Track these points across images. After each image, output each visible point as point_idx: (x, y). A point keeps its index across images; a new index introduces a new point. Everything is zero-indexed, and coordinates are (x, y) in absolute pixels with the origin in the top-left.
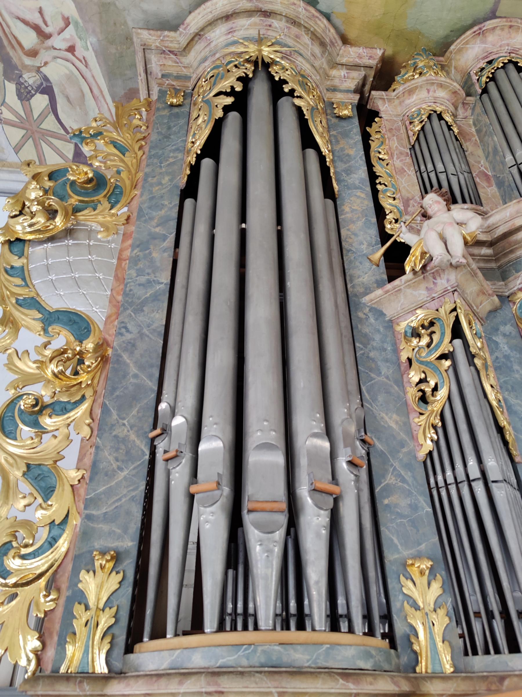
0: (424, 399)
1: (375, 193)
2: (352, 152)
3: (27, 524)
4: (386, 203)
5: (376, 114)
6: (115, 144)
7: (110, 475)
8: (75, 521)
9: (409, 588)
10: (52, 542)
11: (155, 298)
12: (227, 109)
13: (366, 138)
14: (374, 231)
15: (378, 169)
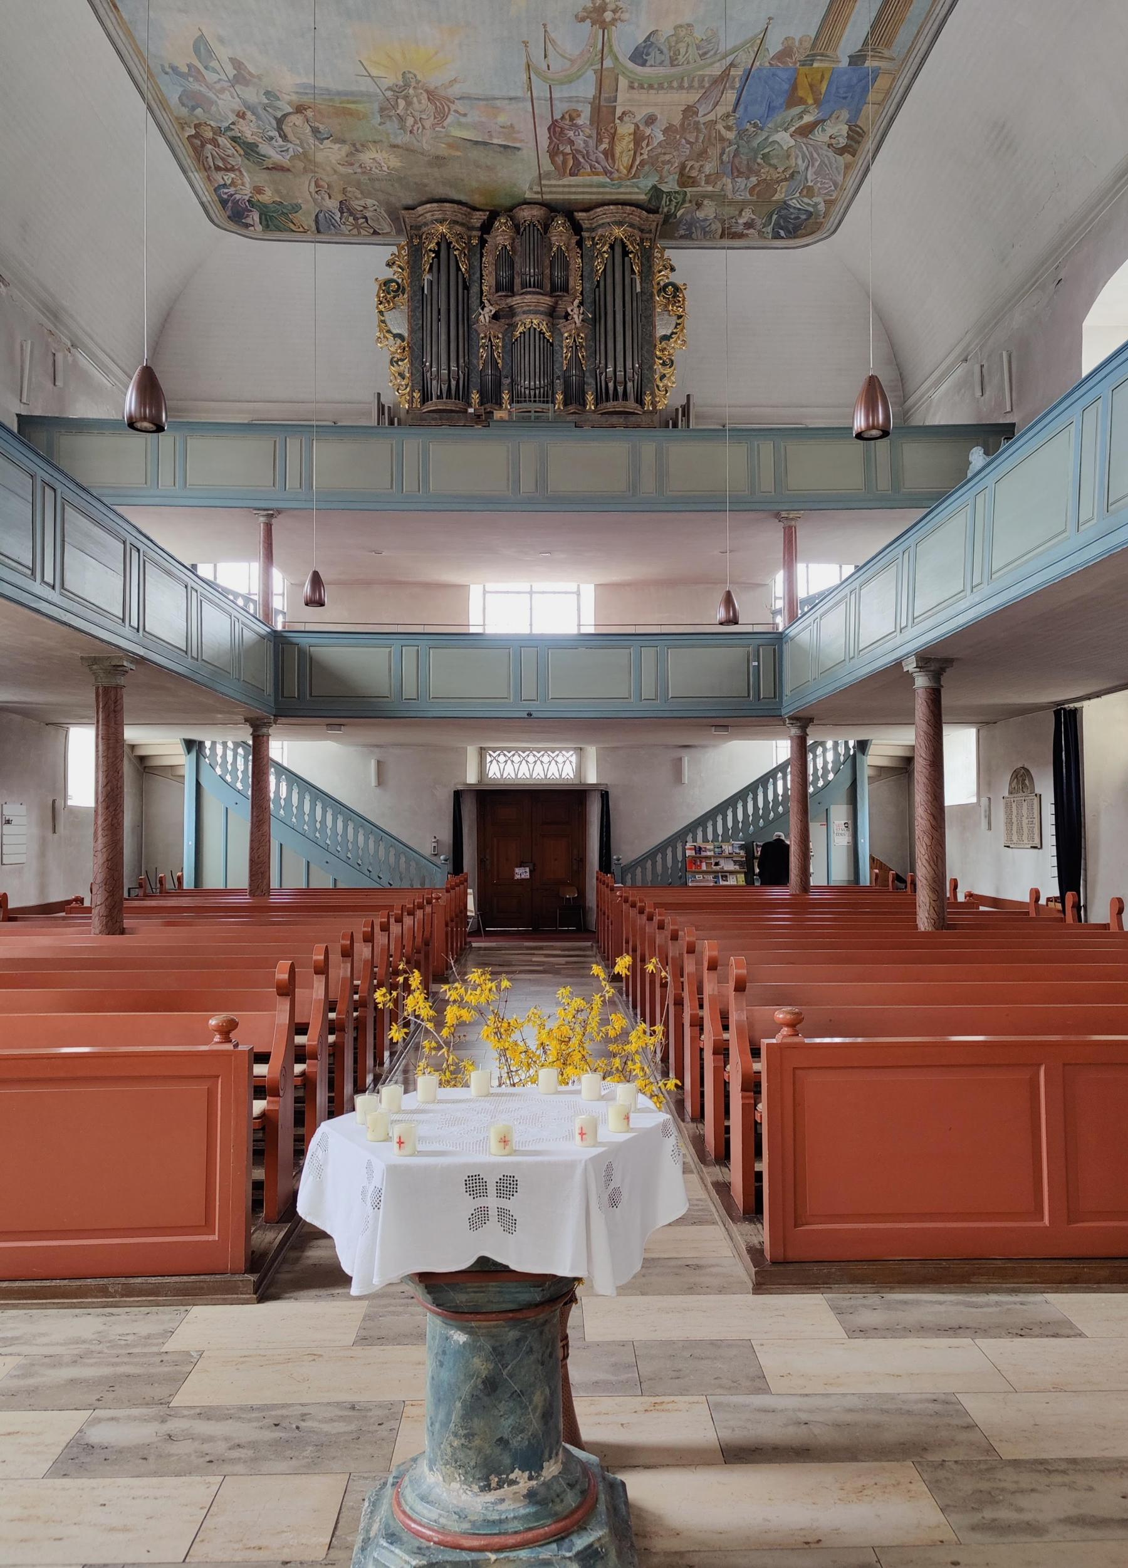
0: (482, 356)
1: (481, 283)
2: (476, 264)
3: (401, 385)
4: (484, 288)
5: (486, 241)
6: (400, 267)
7: (415, 375)
8: (410, 384)
9: (473, 396)
10: (406, 388)
11: (419, 328)
12: (433, 258)
13: (482, 255)
14: (478, 301)
15: (483, 272)
